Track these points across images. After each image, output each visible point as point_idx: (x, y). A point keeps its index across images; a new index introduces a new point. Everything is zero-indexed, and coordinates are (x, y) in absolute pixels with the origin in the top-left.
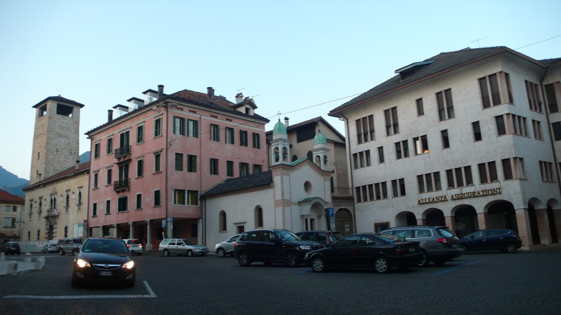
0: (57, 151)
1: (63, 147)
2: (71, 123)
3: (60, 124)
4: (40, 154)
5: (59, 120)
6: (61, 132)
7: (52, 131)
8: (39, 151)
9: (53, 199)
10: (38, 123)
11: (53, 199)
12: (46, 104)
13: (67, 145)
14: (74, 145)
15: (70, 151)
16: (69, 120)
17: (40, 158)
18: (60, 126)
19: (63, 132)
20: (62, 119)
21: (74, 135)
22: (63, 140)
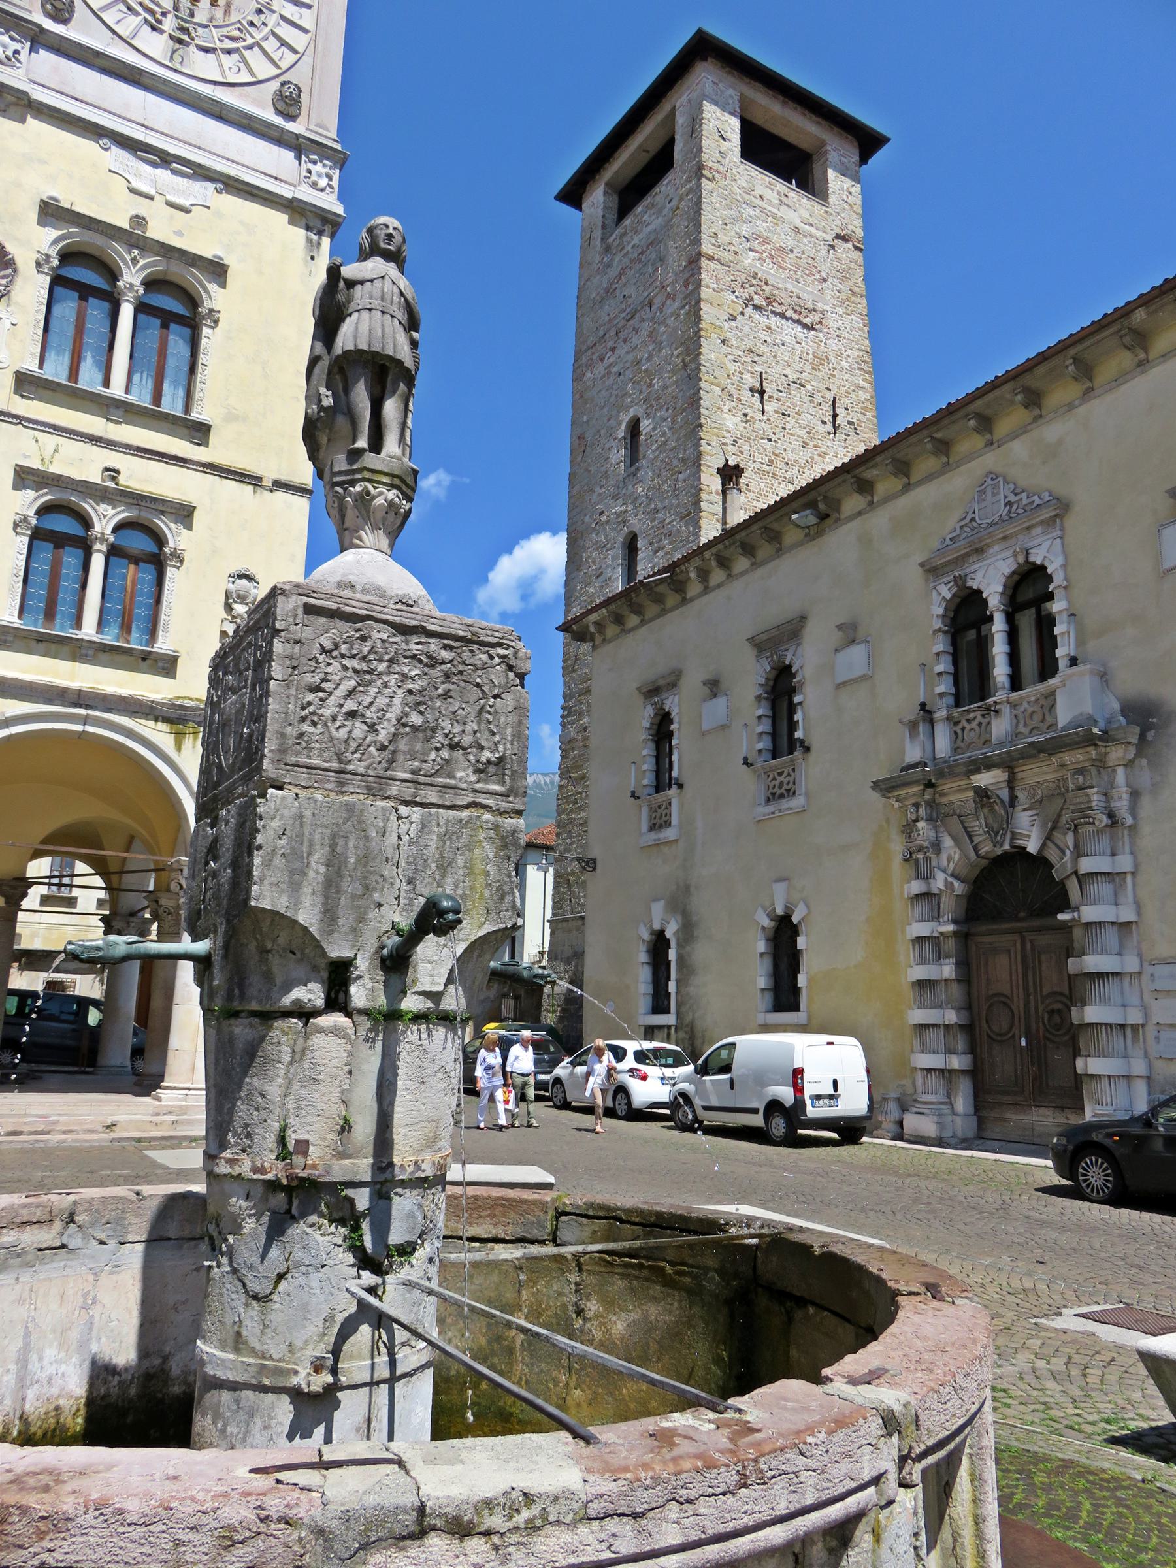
0: (762, 392)
1: (792, 376)
2: (819, 234)
3: (762, 227)
4: (645, 425)
5: (758, 202)
6: (780, 280)
7: (727, 256)
8: (632, 413)
9: (994, 595)
10: (609, 265)
11: (994, 595)
12: (673, 110)
13: (808, 368)
14: (847, 377)
15: (828, 407)
16: (806, 215)
17: (649, 452)
18: (766, 241)
19: (784, 281)
20: (772, 196)
21: (841, 311)
22: (789, 331)
